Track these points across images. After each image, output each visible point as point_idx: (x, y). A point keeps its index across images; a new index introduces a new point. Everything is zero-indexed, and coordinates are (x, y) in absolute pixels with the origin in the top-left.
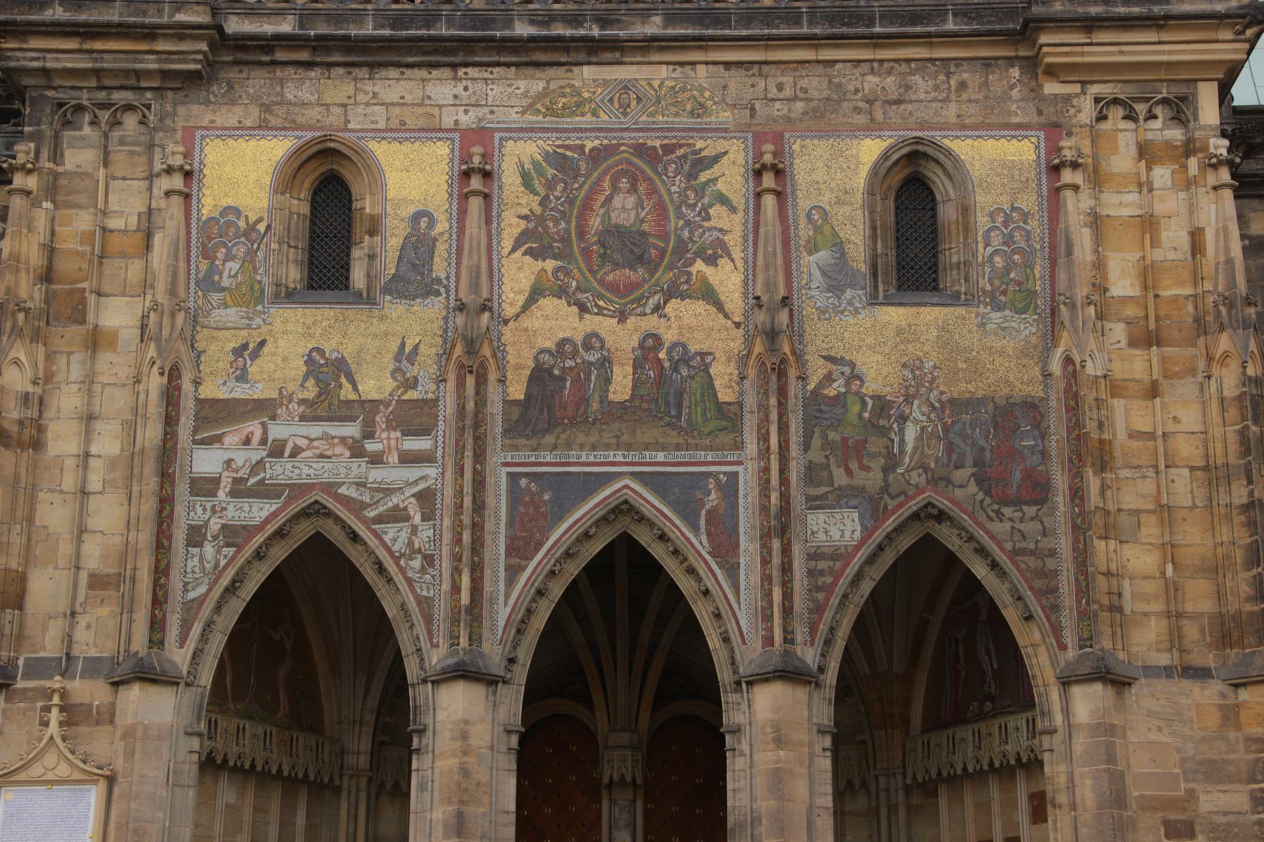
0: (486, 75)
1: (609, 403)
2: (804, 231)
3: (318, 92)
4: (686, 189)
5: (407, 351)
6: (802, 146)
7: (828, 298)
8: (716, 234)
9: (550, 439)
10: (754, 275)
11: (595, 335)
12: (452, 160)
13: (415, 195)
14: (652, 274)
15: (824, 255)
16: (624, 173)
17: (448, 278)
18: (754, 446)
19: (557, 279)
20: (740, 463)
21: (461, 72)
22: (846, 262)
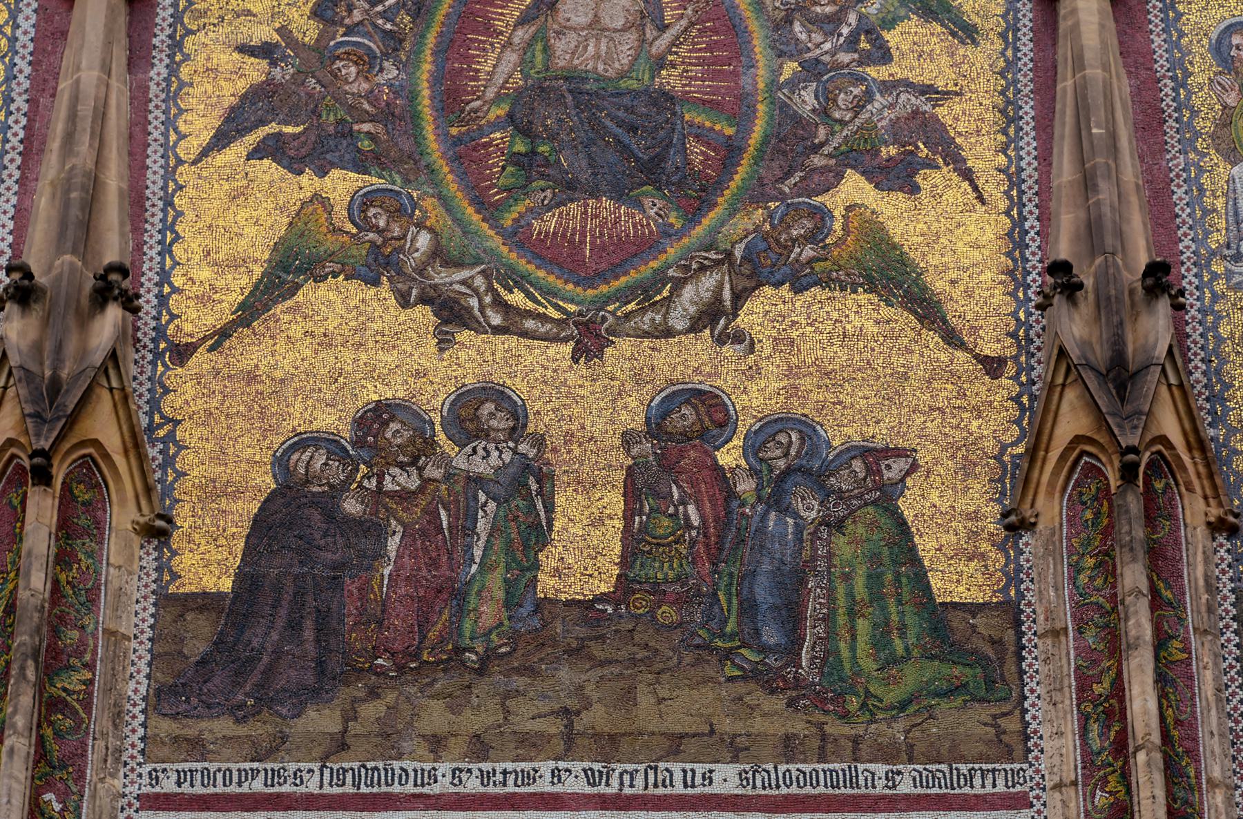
8: (909, 102)
9: (321, 720)
10: (1045, 217)
14: (693, 215)
18: (1070, 744)
19: (365, 225)
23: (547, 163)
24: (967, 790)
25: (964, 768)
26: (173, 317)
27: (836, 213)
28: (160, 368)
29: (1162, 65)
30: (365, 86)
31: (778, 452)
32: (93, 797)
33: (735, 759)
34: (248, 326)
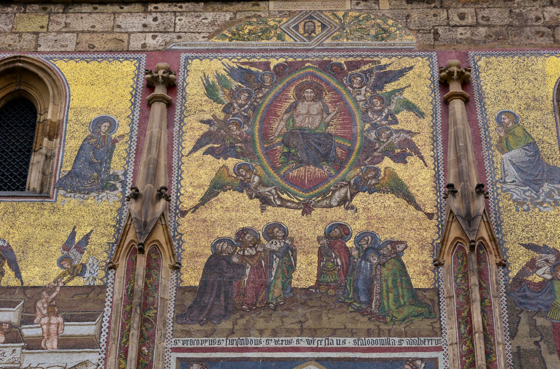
0: (175, 9)
1: (293, 289)
2: (494, 132)
3: (13, 23)
4: (372, 97)
5: (77, 240)
6: (487, 63)
7: (525, 191)
8: (403, 135)
9: (226, 325)
10: (445, 171)
11: (279, 225)
12: (137, 76)
13: (98, 104)
14: (338, 171)
15: (516, 153)
16: (310, 85)
17: (125, 174)
18: (455, 331)
19: (239, 174)
20: (439, 349)
21: (151, 7)
22: (540, 160)
23: (294, 155)
24: (423, 345)
25: (422, 339)
26: (181, 203)
27: (382, 170)
28: (177, 218)
29: (481, 124)
30: (238, 132)
31: (365, 243)
32: (157, 348)
33: (352, 336)
34: (203, 205)
